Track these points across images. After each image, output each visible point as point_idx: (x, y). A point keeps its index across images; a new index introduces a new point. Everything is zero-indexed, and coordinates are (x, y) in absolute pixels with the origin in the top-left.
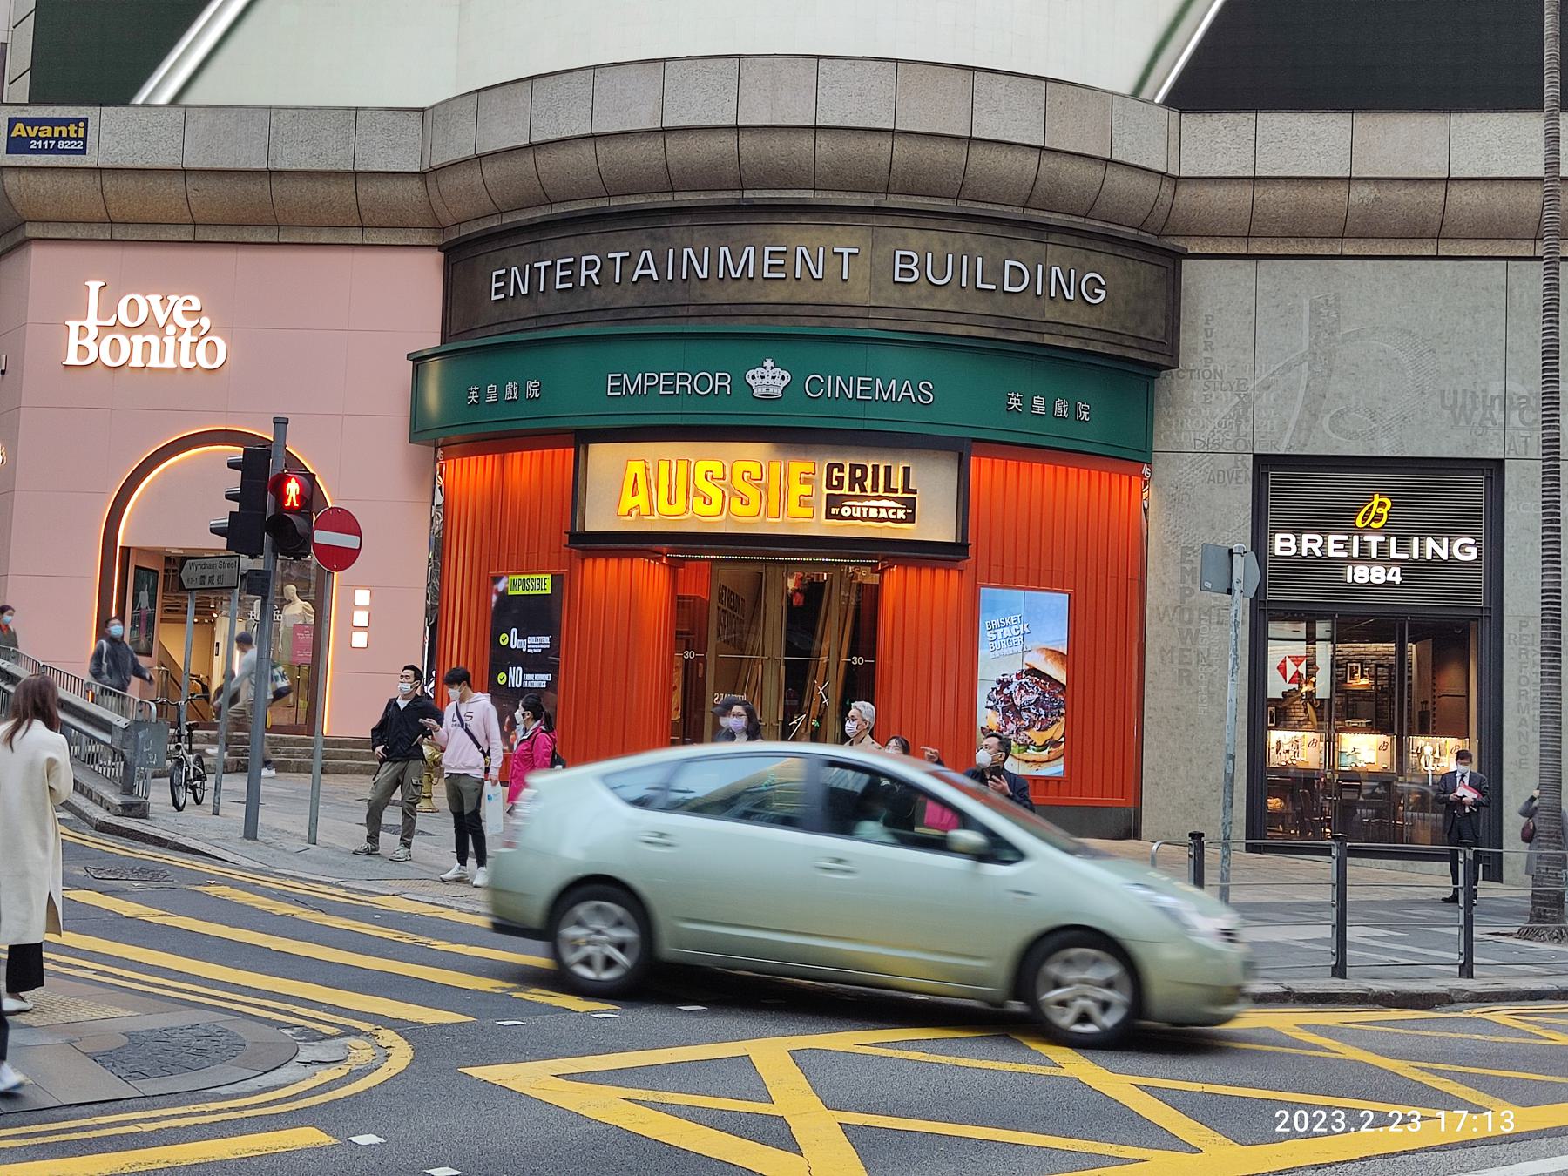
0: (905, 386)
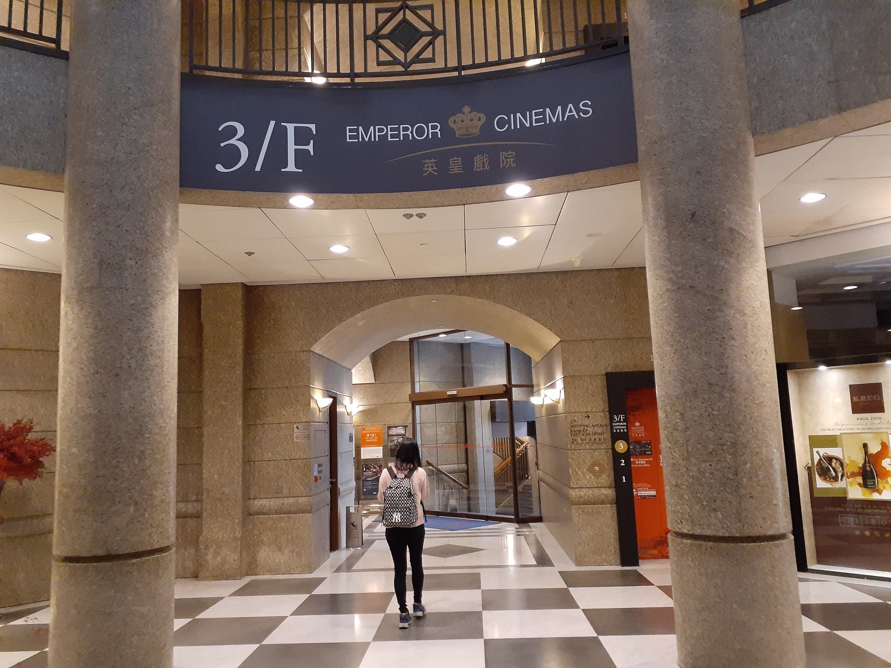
0: (569, 108)
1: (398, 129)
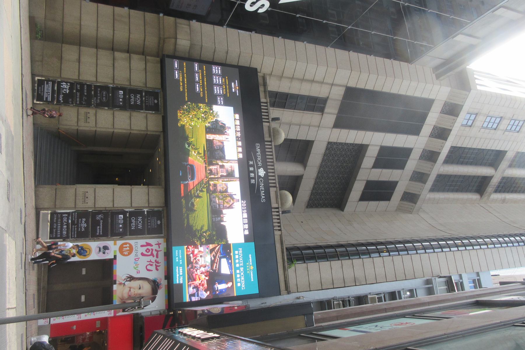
1: (260, 156)
